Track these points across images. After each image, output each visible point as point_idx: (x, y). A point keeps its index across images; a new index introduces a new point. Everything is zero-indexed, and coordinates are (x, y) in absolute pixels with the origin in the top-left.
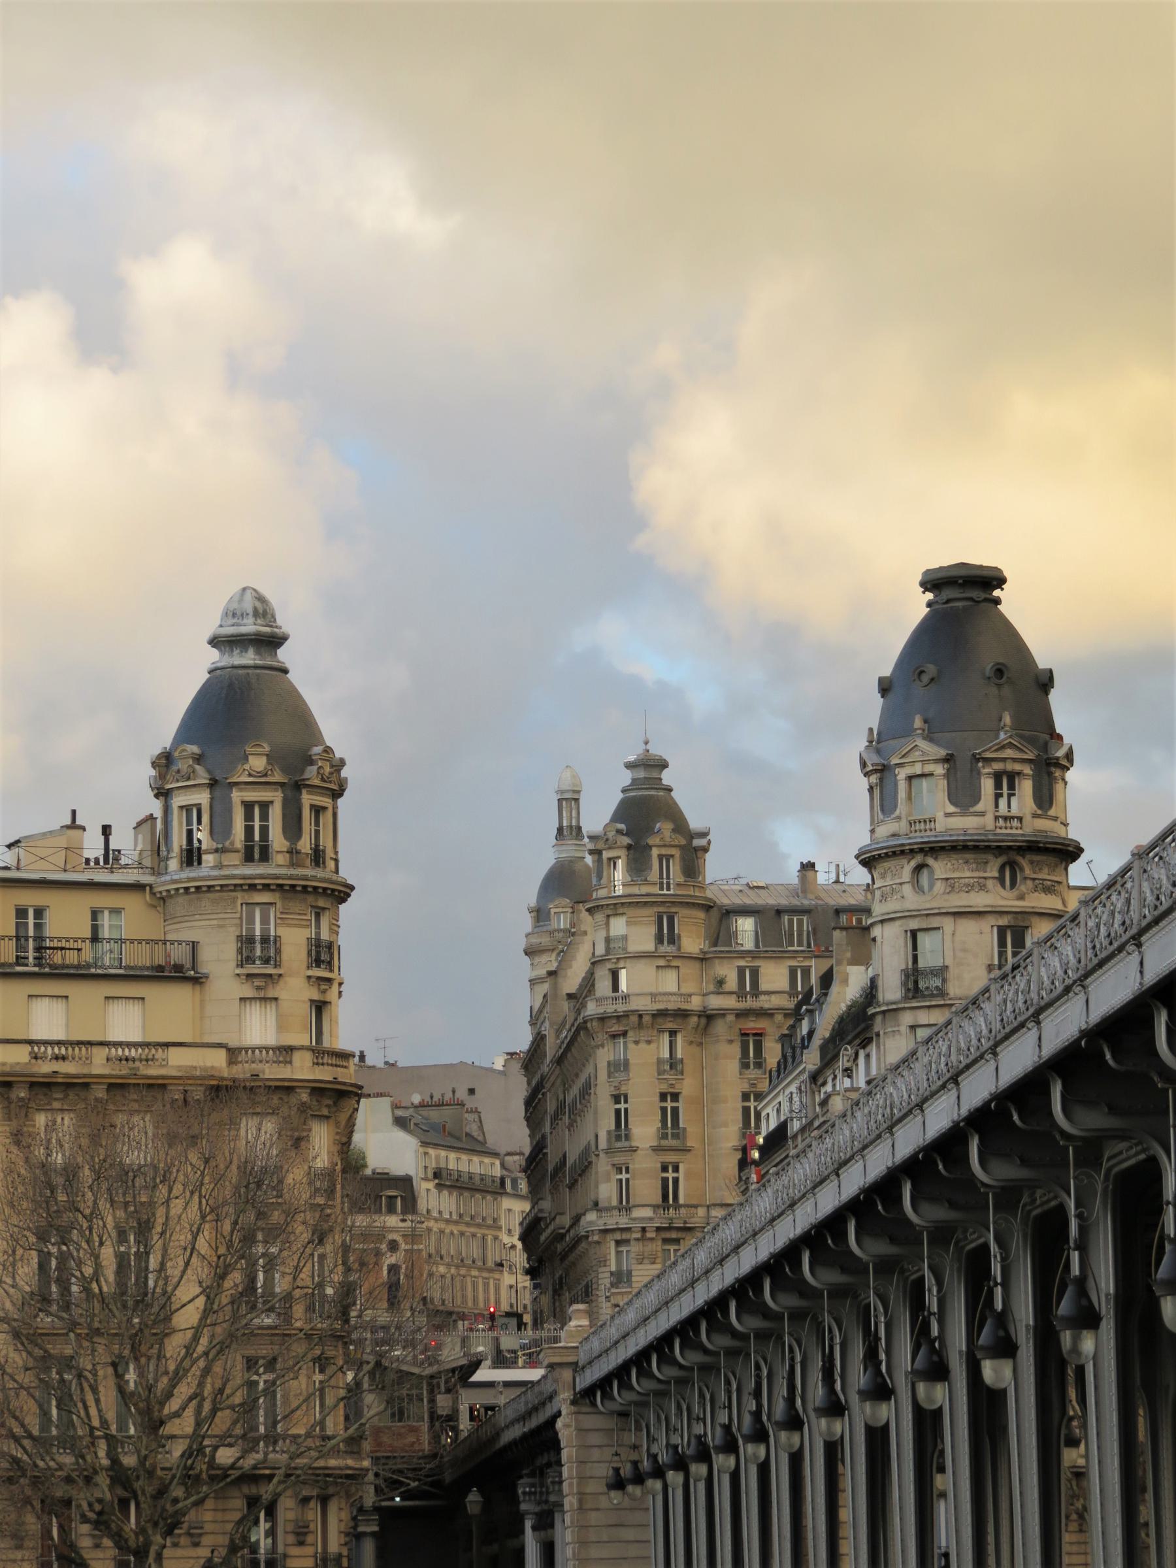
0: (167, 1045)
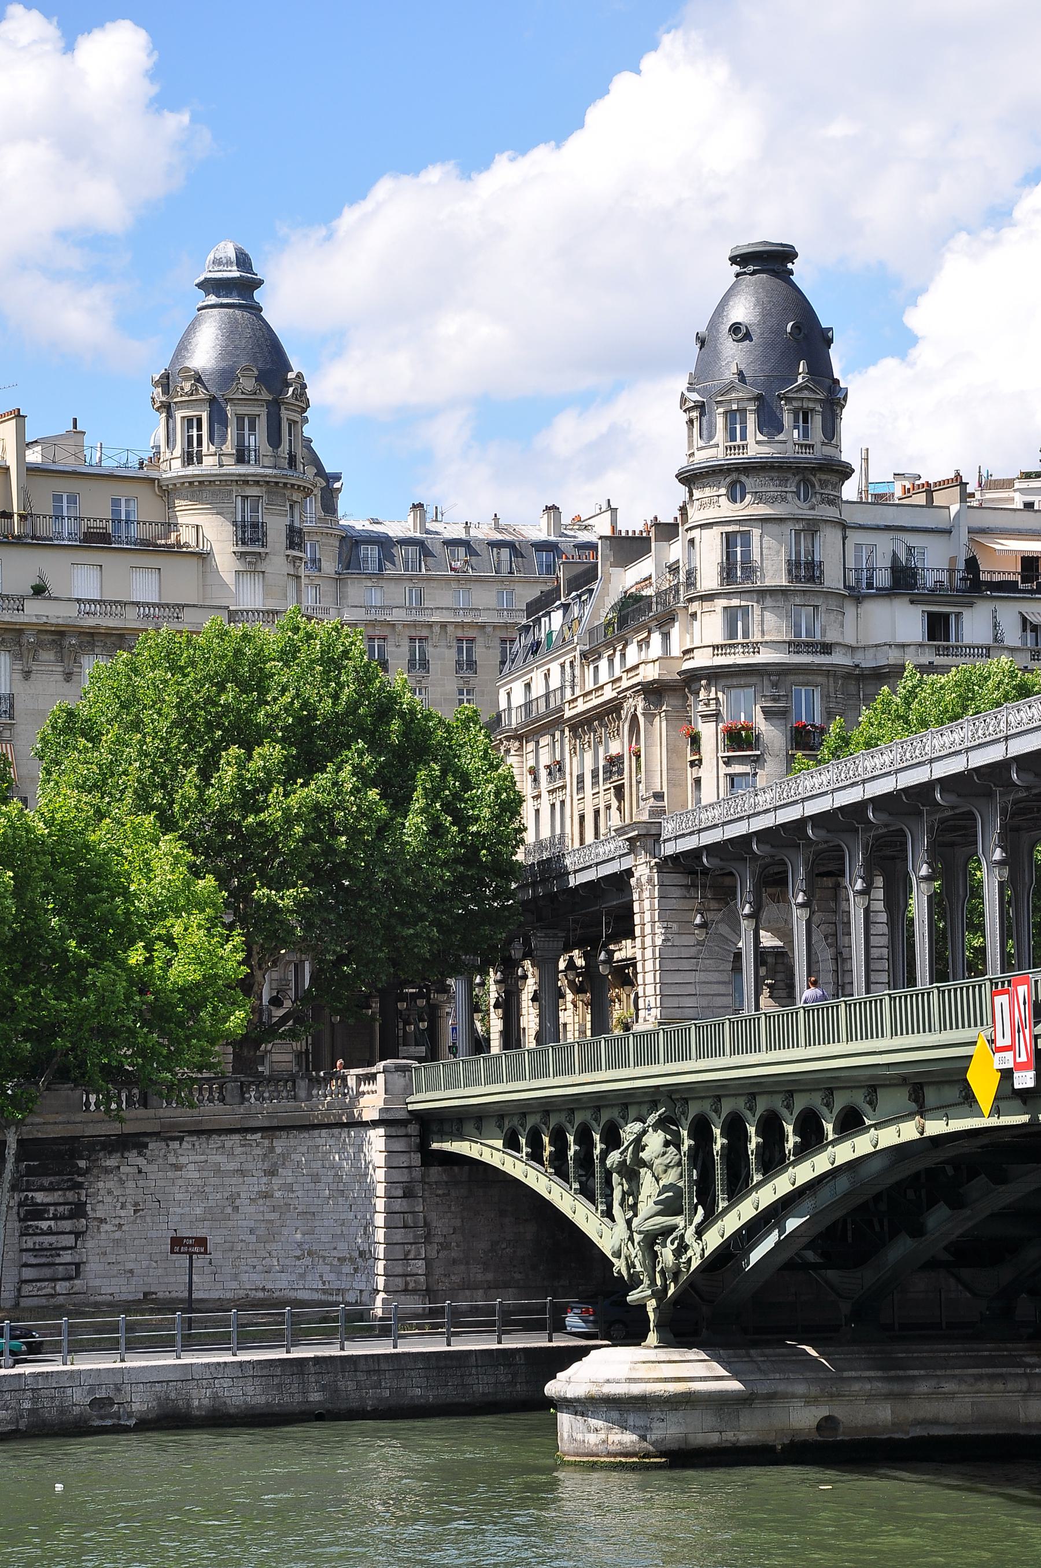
0: (184, 606)
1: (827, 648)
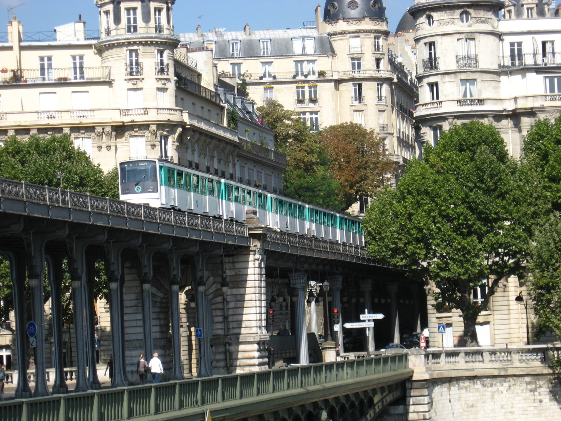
1: (481, 101)
